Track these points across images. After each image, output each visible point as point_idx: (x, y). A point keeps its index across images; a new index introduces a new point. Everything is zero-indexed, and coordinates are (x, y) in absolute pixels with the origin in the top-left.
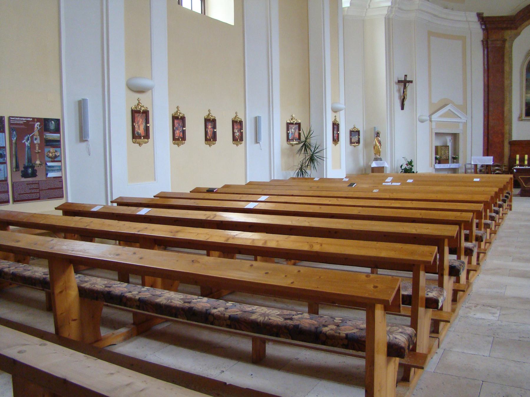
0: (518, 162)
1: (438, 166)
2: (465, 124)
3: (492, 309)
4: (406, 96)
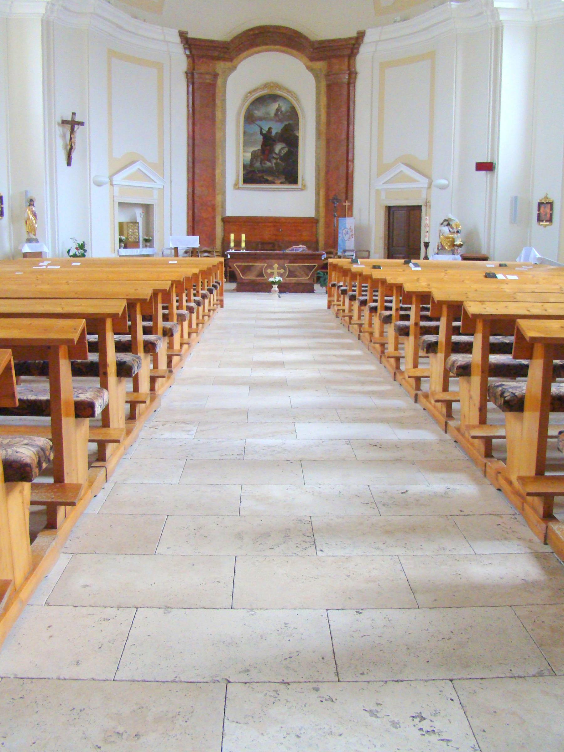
0: (232, 244)
1: (124, 252)
2: (162, 191)
3: (187, 425)
4: (75, 145)
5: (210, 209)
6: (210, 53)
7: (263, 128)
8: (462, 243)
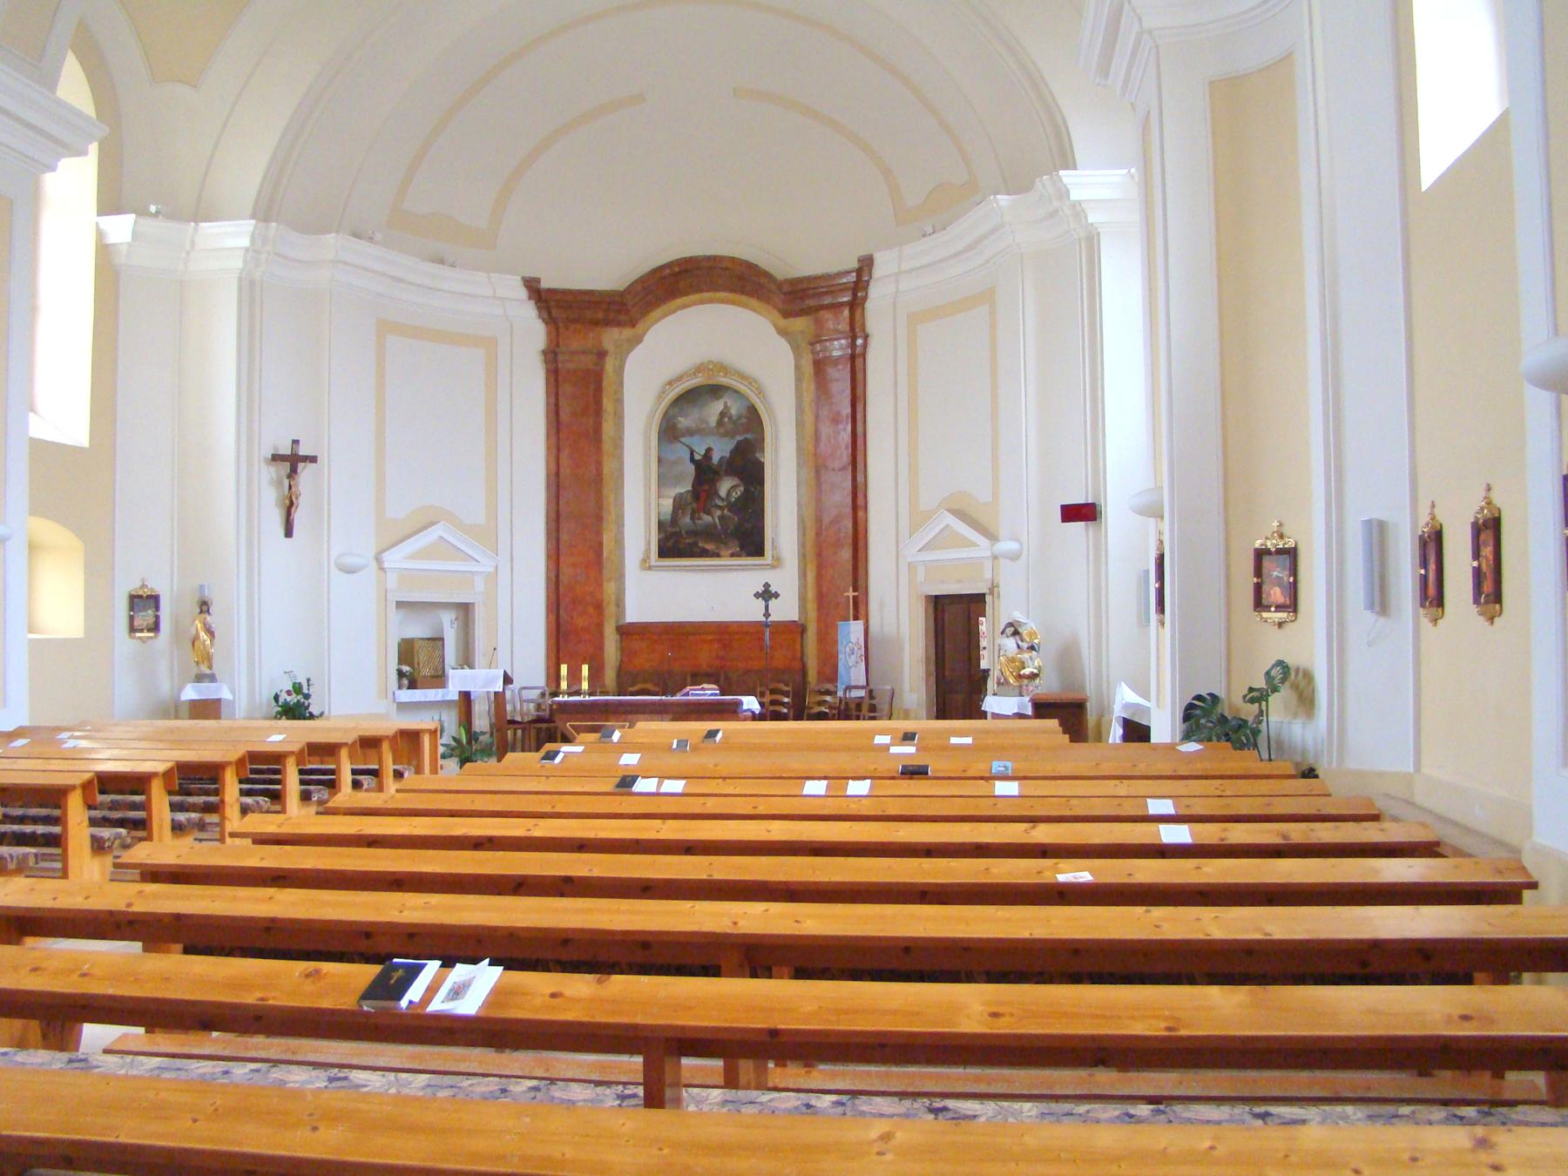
0: (564, 685)
1: (407, 695)
2: (493, 578)
4: (297, 498)
5: (591, 610)
6: (589, 314)
7: (696, 448)
8: (1035, 671)
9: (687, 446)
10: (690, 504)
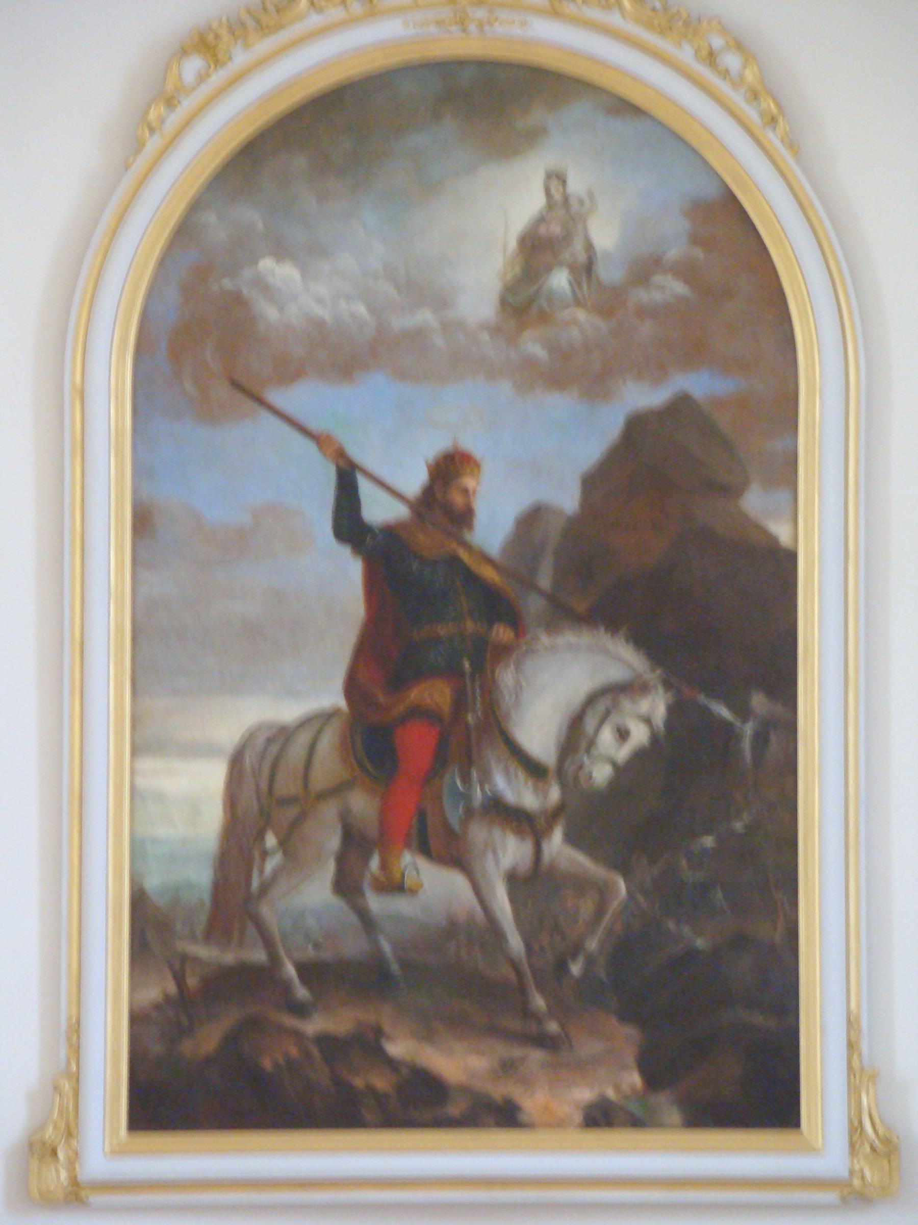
9: (320, 440)
10: (337, 790)
